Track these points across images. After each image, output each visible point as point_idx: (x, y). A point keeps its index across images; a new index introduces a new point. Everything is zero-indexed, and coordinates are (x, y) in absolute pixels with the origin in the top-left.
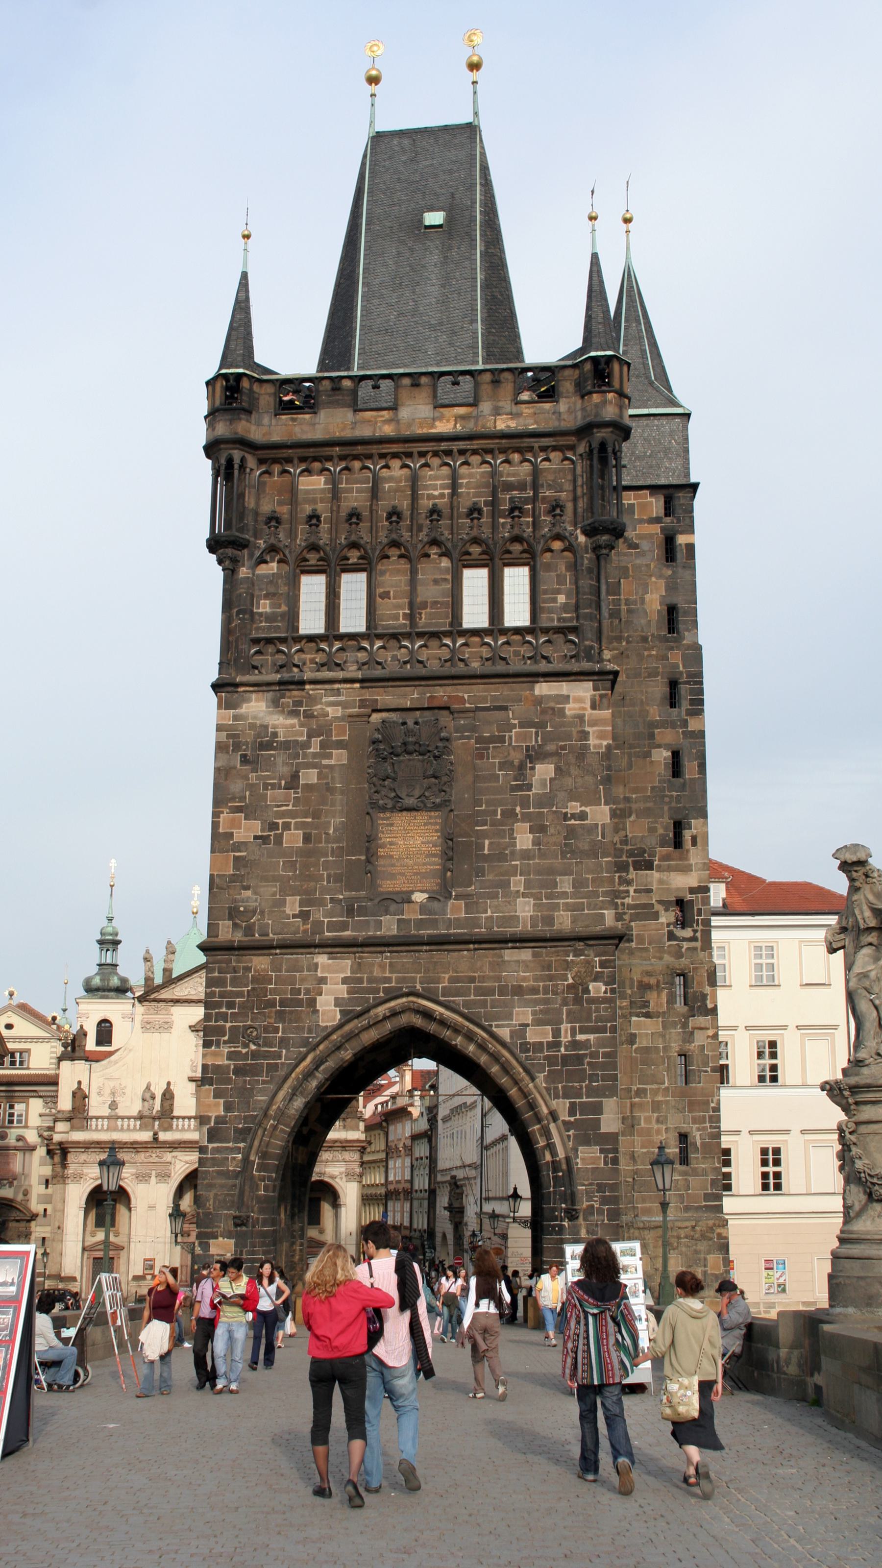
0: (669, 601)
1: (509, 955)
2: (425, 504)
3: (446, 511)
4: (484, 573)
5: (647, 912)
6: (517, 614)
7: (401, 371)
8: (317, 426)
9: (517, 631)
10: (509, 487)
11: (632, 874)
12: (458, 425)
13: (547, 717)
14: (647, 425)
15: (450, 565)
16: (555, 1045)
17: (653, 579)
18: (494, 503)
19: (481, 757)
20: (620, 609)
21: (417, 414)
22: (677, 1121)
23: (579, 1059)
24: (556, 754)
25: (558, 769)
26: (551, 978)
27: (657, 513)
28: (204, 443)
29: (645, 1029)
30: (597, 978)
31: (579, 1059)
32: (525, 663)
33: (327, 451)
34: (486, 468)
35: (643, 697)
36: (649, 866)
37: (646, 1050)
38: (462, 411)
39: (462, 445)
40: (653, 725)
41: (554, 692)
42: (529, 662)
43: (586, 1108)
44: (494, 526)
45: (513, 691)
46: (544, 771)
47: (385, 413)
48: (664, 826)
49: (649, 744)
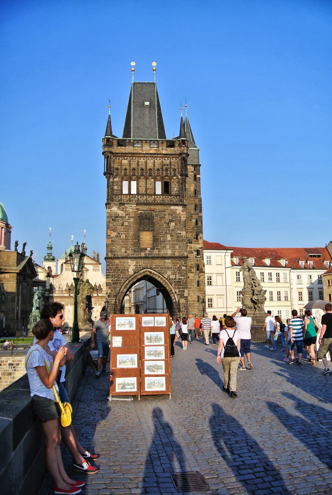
1: (166, 261)
2: (148, 168)
5: (191, 252)
10: (165, 165)
11: (188, 244)
16: (176, 279)
18: (162, 168)
19: (160, 221)
21: (146, 148)
22: (197, 294)
23: (180, 282)
24: (175, 221)
25: (175, 224)
26: (175, 266)
29: (191, 275)
30: (183, 266)
31: (180, 282)
36: (192, 243)
37: (192, 280)
38: (156, 148)
40: (192, 214)
43: (181, 291)
44: (162, 173)
46: (173, 224)
48: (194, 235)
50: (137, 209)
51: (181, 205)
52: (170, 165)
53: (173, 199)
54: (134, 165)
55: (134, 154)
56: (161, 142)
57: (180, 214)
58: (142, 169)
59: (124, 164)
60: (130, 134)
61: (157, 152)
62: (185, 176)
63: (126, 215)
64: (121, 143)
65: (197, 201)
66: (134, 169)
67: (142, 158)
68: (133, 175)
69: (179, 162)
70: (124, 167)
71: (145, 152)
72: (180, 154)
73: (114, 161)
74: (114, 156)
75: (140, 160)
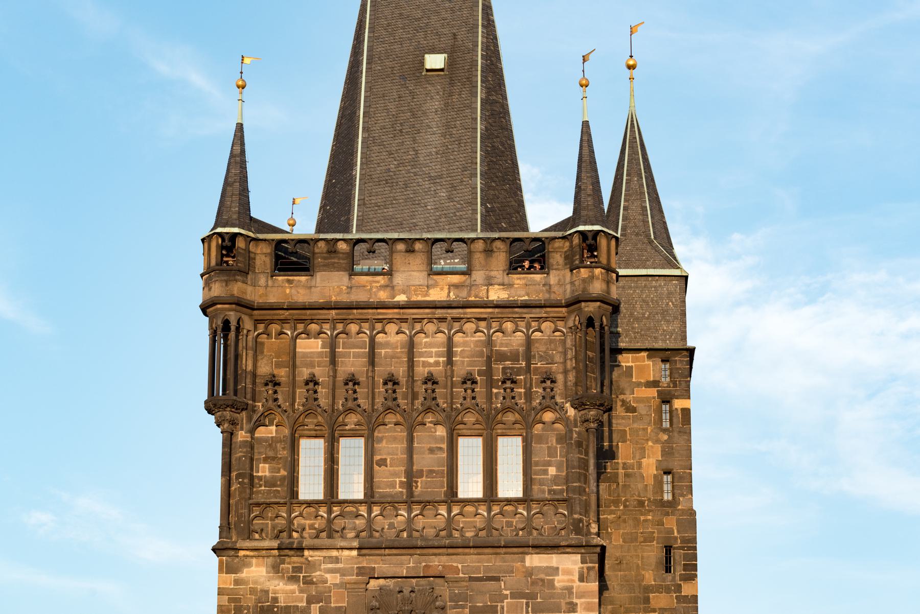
0: (665, 466)
2: (421, 371)
3: (441, 379)
4: (478, 442)
6: (510, 485)
7: (395, 236)
8: (313, 289)
9: (509, 501)
10: (502, 357)
12: (452, 294)
13: (537, 589)
14: (645, 286)
15: (445, 434)
17: (650, 443)
20: (617, 474)
27: (654, 376)
28: (200, 302)
32: (517, 535)
33: (323, 314)
34: (480, 337)
35: (640, 562)
38: (455, 279)
39: (455, 312)
40: (648, 589)
41: (545, 565)
42: (521, 533)
44: (489, 397)
45: (505, 562)
47: (379, 278)
49: (644, 608)
50: (361, 571)
51: (574, 547)
52: (528, 357)
53: (538, 521)
54: (352, 362)
55: (349, 307)
56: (480, 245)
57: (569, 589)
58: (392, 381)
59: (305, 355)
60: (349, 212)
61: (463, 295)
62: (594, 406)
63: (309, 602)
64: (291, 257)
65: (671, 523)
66: (352, 380)
67: (392, 328)
68: (350, 410)
69: (569, 343)
70: (304, 373)
71: (401, 298)
72: (573, 303)
73: (257, 348)
74: (257, 322)
75: (380, 338)
